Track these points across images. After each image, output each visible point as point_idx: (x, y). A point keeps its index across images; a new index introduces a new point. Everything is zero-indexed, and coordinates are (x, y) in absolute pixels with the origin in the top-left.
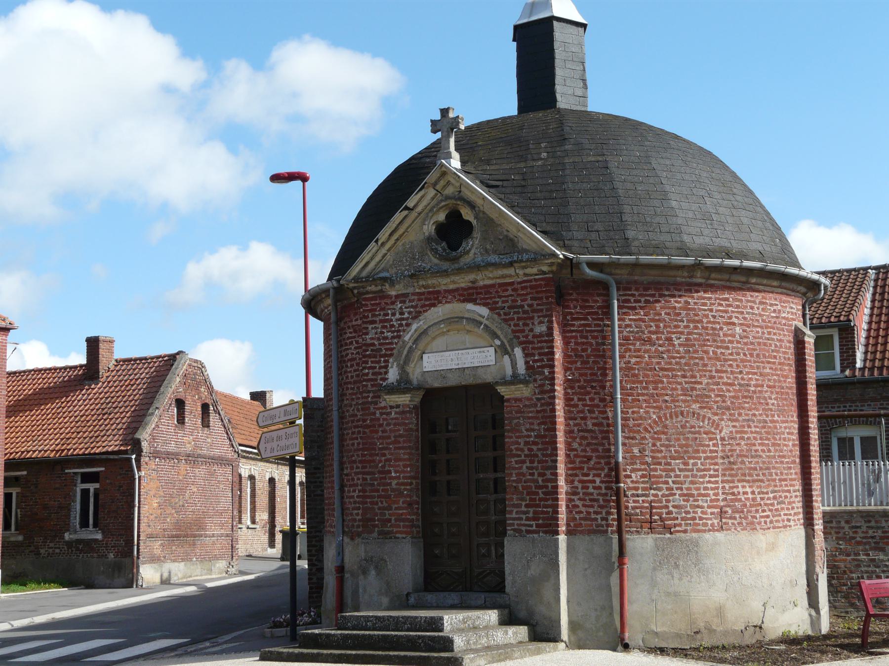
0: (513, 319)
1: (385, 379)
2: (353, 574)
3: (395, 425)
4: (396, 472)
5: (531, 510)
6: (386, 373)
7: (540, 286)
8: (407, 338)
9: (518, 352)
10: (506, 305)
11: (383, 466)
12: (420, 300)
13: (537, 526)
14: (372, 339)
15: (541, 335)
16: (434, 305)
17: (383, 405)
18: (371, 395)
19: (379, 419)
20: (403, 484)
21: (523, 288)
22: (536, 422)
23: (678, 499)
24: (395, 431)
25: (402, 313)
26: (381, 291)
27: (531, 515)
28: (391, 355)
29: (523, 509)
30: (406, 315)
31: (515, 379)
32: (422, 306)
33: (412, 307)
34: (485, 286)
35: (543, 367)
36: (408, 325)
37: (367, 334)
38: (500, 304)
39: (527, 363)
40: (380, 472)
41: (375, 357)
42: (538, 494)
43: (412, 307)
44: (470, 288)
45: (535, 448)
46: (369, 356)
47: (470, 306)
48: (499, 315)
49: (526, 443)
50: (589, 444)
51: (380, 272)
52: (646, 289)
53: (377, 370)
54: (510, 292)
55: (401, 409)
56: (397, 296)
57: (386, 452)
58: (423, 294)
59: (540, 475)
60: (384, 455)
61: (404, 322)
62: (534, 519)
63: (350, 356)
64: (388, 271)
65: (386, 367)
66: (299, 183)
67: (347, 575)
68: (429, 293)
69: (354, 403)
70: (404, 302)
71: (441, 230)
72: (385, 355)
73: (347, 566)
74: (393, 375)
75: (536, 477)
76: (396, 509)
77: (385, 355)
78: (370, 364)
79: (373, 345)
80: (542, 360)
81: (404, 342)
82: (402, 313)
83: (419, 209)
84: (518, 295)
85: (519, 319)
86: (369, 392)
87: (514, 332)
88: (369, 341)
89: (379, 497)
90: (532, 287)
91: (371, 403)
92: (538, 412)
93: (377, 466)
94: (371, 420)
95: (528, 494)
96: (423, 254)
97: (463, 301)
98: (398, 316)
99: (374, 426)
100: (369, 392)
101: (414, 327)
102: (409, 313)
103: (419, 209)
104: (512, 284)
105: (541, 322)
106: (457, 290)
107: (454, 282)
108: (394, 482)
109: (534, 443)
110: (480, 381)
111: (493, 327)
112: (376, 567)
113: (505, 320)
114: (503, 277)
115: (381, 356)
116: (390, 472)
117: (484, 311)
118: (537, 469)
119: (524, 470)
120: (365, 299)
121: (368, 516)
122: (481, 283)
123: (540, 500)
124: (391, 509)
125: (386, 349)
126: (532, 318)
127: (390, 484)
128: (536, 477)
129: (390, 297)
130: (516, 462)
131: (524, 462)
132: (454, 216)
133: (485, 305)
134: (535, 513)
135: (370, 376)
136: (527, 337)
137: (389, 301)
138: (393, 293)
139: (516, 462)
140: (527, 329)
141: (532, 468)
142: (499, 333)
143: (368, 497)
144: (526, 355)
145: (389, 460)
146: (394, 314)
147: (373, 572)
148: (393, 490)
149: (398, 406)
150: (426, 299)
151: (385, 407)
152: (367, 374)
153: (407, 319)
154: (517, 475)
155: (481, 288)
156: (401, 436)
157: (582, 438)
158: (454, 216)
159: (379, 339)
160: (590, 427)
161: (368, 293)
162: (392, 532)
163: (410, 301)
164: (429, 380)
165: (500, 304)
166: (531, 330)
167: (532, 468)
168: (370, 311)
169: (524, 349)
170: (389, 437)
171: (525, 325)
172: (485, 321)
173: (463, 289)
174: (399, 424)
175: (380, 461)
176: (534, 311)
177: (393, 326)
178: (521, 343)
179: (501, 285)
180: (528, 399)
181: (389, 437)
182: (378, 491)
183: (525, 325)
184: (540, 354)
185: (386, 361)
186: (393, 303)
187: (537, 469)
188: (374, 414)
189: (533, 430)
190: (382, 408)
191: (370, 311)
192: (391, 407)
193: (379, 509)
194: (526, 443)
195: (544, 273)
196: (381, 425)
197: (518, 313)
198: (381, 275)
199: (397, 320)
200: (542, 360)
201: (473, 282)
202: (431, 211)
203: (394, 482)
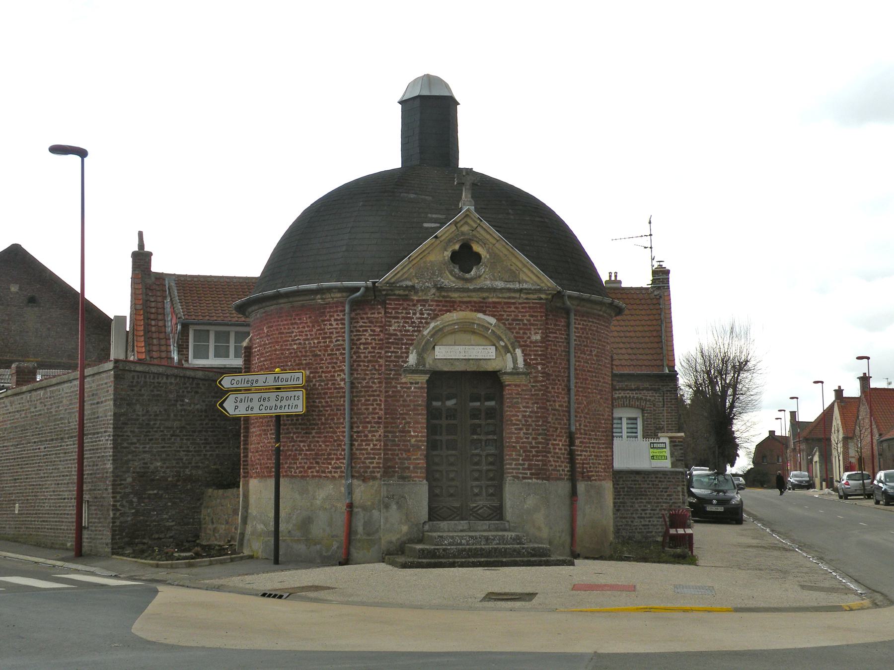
0: (515, 328)
1: (406, 362)
2: (364, 508)
3: (414, 396)
4: (414, 432)
5: (527, 463)
6: (407, 357)
7: (536, 308)
8: (425, 333)
9: (518, 352)
10: (510, 318)
11: (404, 427)
12: (437, 306)
13: (531, 474)
14: (394, 330)
15: (536, 342)
16: (450, 311)
17: (404, 380)
18: (393, 373)
19: (399, 392)
20: (420, 441)
21: (523, 308)
22: (530, 402)
23: (286, 466)
24: (414, 401)
25: (422, 314)
26: (407, 295)
27: (526, 466)
28: (412, 344)
29: (521, 462)
30: (425, 316)
31: (515, 373)
32: (440, 311)
33: (431, 310)
34: (494, 303)
35: (537, 364)
36: (427, 323)
37: (390, 326)
38: (505, 317)
39: (525, 360)
40: (400, 432)
41: (397, 344)
42: (531, 452)
43: (431, 310)
44: (481, 302)
45: (530, 420)
46: (392, 343)
47: (480, 315)
48: (505, 324)
49: (524, 416)
50: (556, 419)
51: (403, 280)
52: (583, 316)
53: (399, 354)
54: (513, 309)
55: (419, 385)
56: (418, 301)
57: (407, 417)
58: (441, 301)
59: (533, 438)
60: (404, 419)
61: (424, 321)
62: (529, 469)
63: (363, 341)
64: (410, 280)
65: (407, 353)
66: (77, 159)
67: (355, 510)
68: (446, 301)
69: (367, 377)
70: (424, 306)
71: (455, 257)
72: (406, 344)
73: (356, 503)
74: (412, 359)
75: (530, 440)
76: (415, 459)
77: (406, 344)
78: (392, 350)
79: (396, 335)
80: (536, 359)
81: (423, 335)
82: (422, 314)
83: (443, 238)
84: (520, 312)
85: (520, 329)
86: (391, 370)
87: (515, 337)
88: (392, 332)
89: (399, 450)
90: (529, 307)
91: (393, 379)
92: (532, 395)
93: (398, 427)
94: (393, 392)
95: (524, 452)
96: (441, 274)
97: (475, 311)
98: (418, 315)
99: (395, 396)
100: (391, 370)
101: (432, 325)
102: (428, 314)
103: (443, 238)
104: (514, 303)
105: (536, 333)
106: (470, 302)
107: (469, 297)
108: (413, 440)
109: (530, 417)
110: (482, 370)
111: (498, 333)
112: (398, 503)
113: (510, 329)
114: (509, 298)
115: (402, 344)
116: (410, 432)
117: (493, 321)
118: (531, 434)
119: (522, 435)
120: (390, 299)
121: (389, 464)
122: (490, 300)
123: (533, 456)
124: (410, 459)
125: (407, 340)
126: (530, 329)
127: (409, 441)
128: (530, 440)
129: (412, 300)
130: (516, 429)
131: (521, 429)
132: (466, 247)
133: (493, 316)
134: (529, 465)
135: (393, 358)
136: (525, 341)
137: (411, 304)
138: (415, 298)
139: (516, 429)
140: (526, 336)
141: (527, 434)
142: (503, 337)
143: (390, 450)
144: (525, 355)
145: (409, 423)
146: (415, 314)
147: (394, 507)
148: (412, 446)
149: (417, 383)
150: (443, 306)
151: (405, 383)
152: (390, 357)
153: (426, 318)
154: (516, 438)
155: (490, 303)
156: (419, 405)
157: (554, 415)
158: (466, 247)
159: (401, 331)
160: (557, 407)
161: (395, 295)
162: (410, 477)
163: (429, 305)
164: (439, 365)
165: (505, 317)
166: (529, 338)
167: (527, 434)
168: (394, 309)
169: (523, 352)
170: (409, 406)
171: (525, 333)
172: (492, 328)
173: (475, 302)
174: (418, 396)
175: (401, 423)
176: (531, 324)
177: (414, 322)
178: (521, 346)
179: (506, 303)
180: (525, 385)
181: (409, 406)
182: (398, 445)
183: (525, 333)
184: (535, 355)
185: (408, 348)
186: (414, 305)
187: (531, 434)
188: (396, 387)
189: (528, 407)
190: (403, 383)
191: (394, 309)
192: (411, 383)
193: (399, 459)
194: (524, 416)
195: (541, 299)
196: (402, 396)
197: (519, 324)
198: (404, 284)
199: (417, 318)
200: (536, 359)
201: (484, 298)
202: (450, 241)
203: (413, 440)
